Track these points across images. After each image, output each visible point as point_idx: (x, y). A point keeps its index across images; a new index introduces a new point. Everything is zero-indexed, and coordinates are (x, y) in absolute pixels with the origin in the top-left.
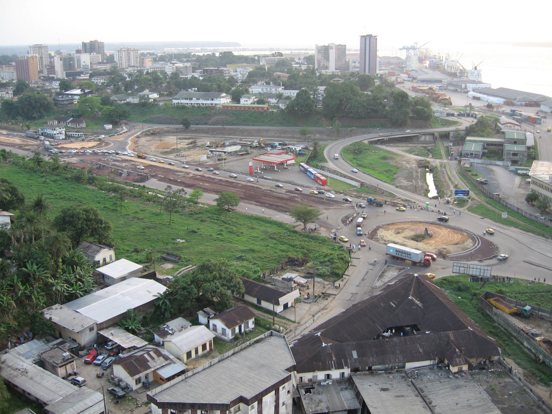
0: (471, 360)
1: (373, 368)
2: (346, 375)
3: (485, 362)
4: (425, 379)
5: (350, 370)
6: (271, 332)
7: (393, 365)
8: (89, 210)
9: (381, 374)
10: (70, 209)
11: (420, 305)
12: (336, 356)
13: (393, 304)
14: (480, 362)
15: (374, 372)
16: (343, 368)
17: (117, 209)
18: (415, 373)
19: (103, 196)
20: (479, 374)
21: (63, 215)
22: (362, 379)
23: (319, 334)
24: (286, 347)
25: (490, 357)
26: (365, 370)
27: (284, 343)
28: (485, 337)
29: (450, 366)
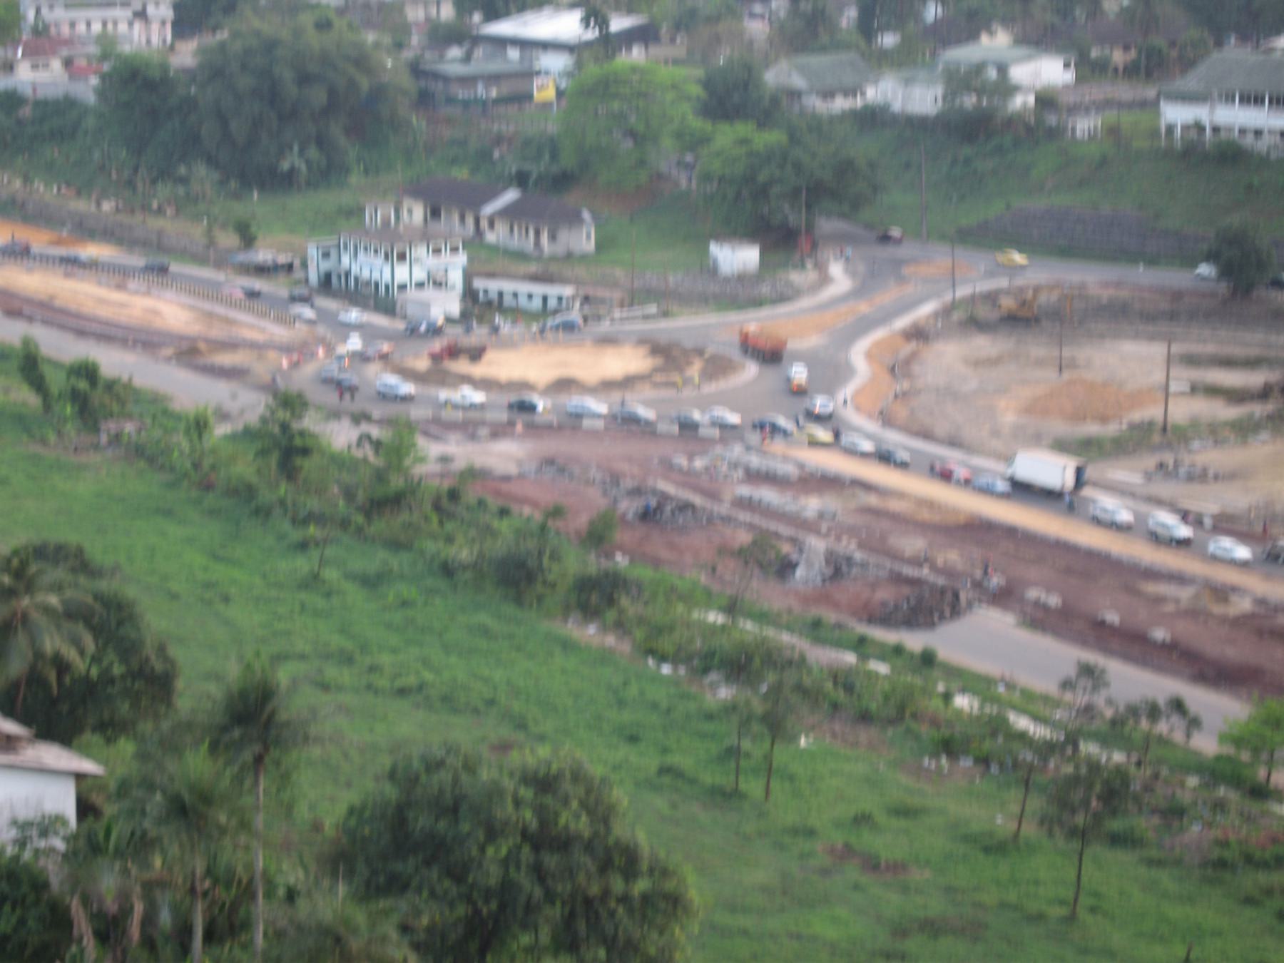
8: (558, 777)
10: (440, 764)
17: (743, 786)
19: (659, 694)
21: (391, 792)
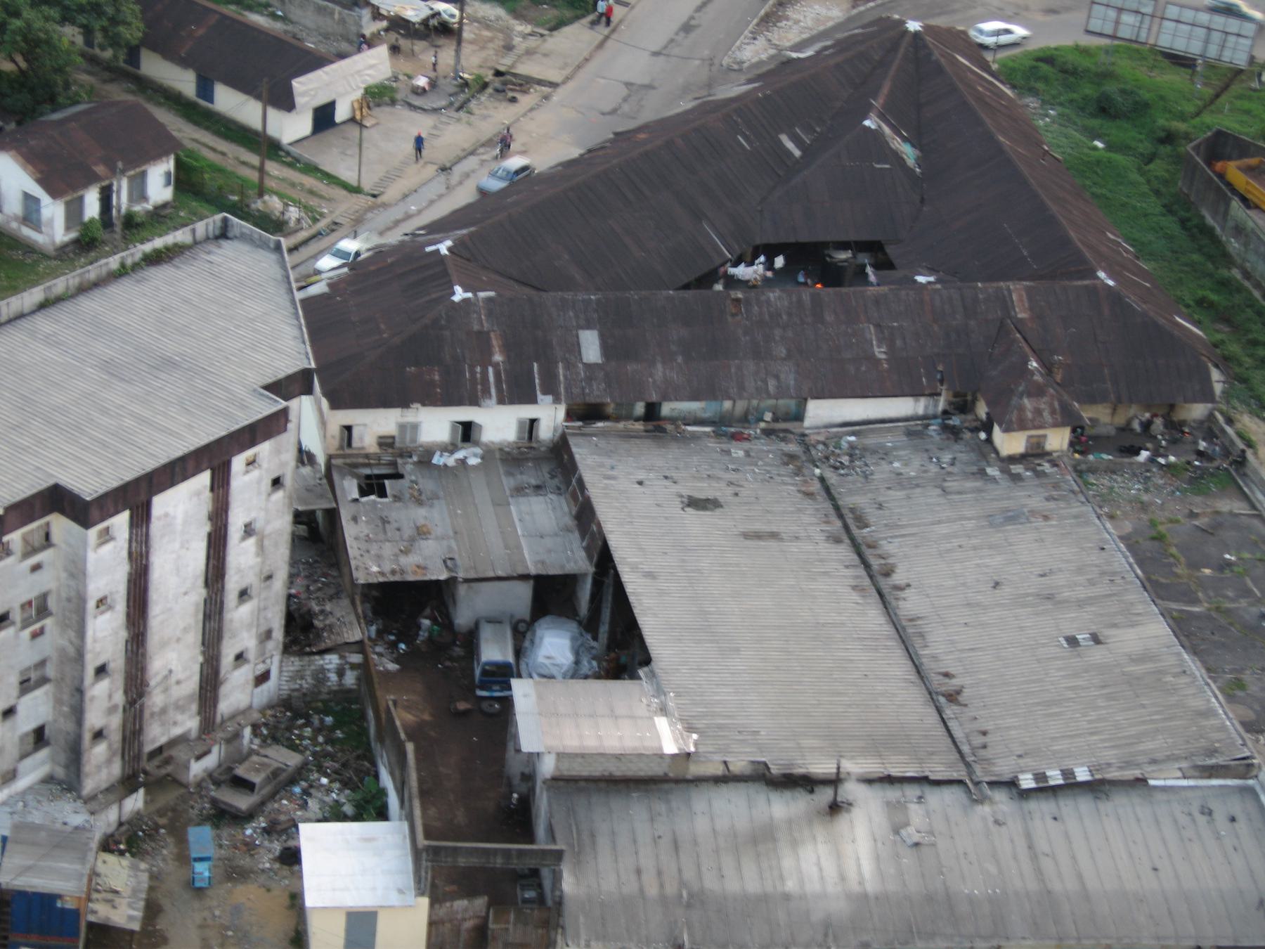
0: (1087, 413)
1: (667, 409)
2: (546, 432)
3: (1146, 426)
4: (881, 471)
5: (561, 412)
6: (225, 220)
7: (755, 402)
9: (695, 437)
11: (911, 162)
12: (507, 348)
13: (790, 145)
14: (1129, 422)
15: (669, 427)
16: (532, 400)
18: (844, 445)
20: (1114, 472)
22: (608, 454)
23: (443, 248)
24: (283, 291)
25: (1172, 407)
26: (629, 417)
27: (276, 272)
28: (1162, 321)
29: (996, 429)
